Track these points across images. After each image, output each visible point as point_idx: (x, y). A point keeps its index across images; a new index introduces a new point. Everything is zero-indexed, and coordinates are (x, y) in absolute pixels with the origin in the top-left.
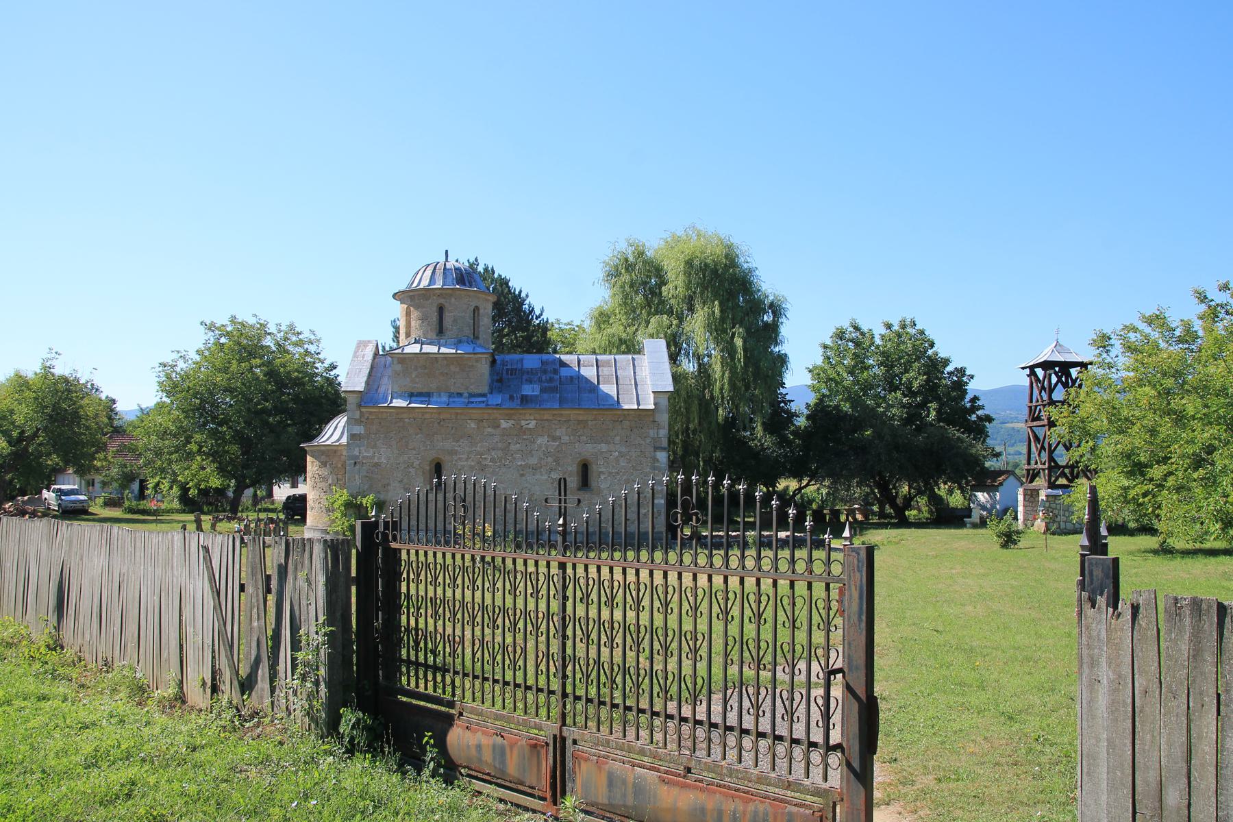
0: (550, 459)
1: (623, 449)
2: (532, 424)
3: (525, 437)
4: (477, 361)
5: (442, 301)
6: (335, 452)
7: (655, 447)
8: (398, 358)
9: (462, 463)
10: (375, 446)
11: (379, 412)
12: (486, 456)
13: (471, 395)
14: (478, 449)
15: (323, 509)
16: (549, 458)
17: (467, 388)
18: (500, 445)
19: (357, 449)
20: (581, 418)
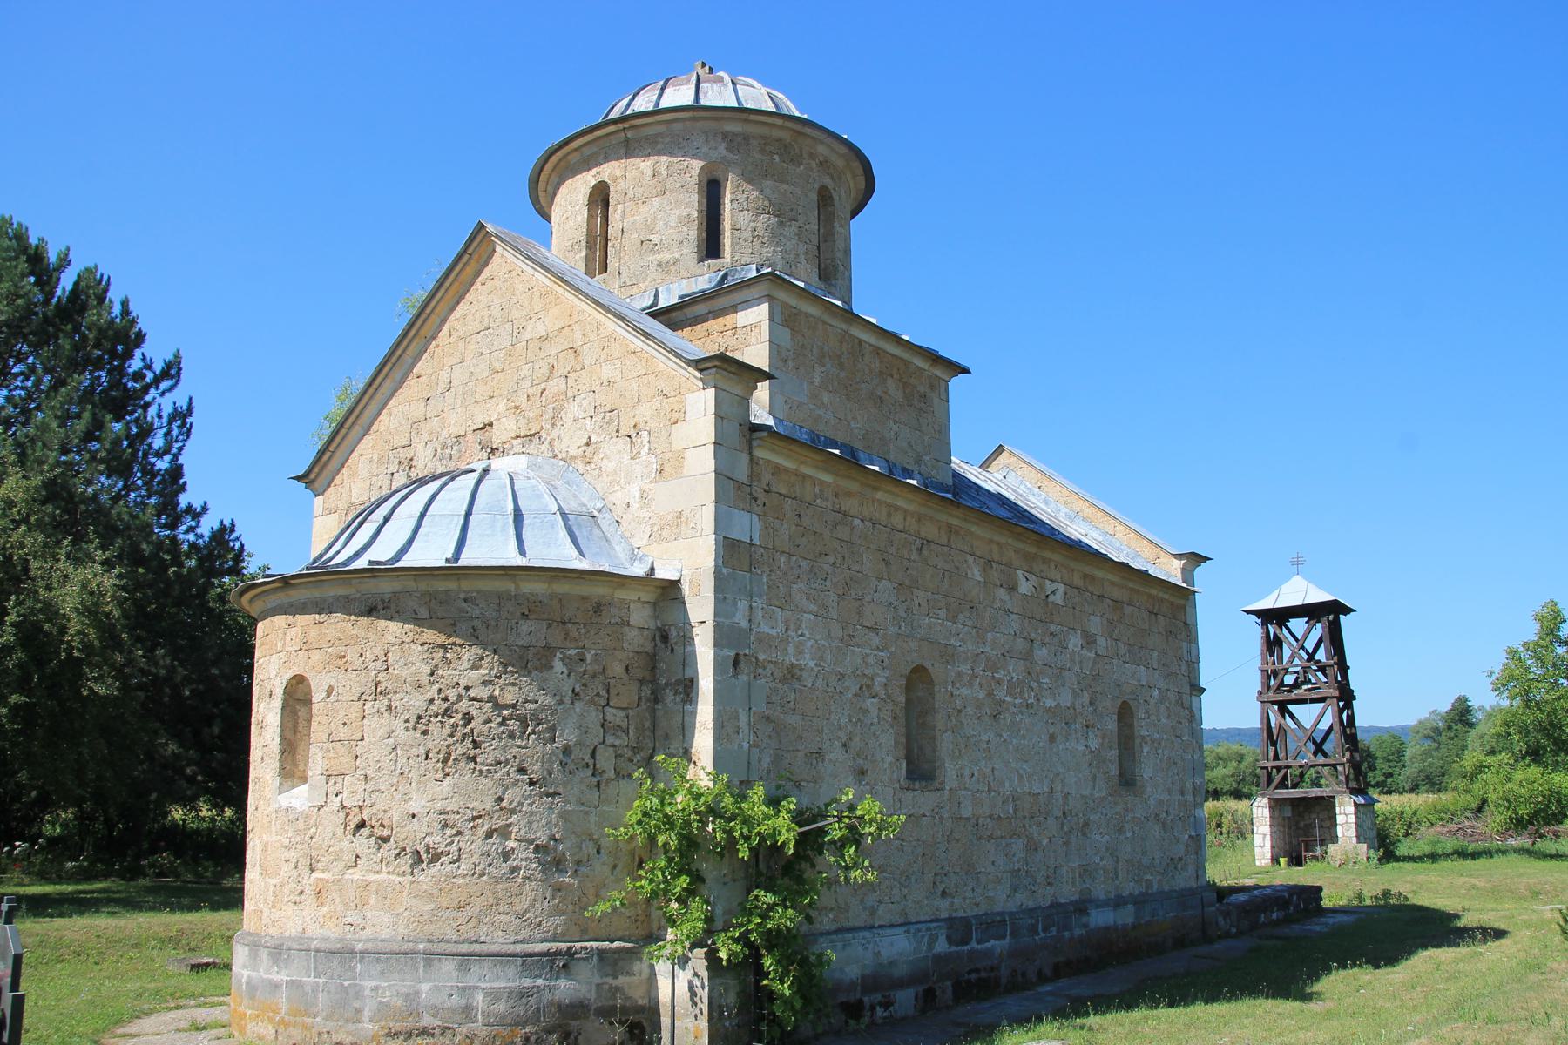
0: (1086, 697)
1: (1163, 686)
2: (1058, 599)
3: (1053, 628)
5: (828, 181)
6: (598, 608)
7: (1191, 686)
8: (785, 305)
9: (965, 691)
14: (987, 649)
15: (523, 857)
16: (1085, 692)
17: (918, 461)
18: (1021, 644)
19: (743, 605)
20: (1117, 594)
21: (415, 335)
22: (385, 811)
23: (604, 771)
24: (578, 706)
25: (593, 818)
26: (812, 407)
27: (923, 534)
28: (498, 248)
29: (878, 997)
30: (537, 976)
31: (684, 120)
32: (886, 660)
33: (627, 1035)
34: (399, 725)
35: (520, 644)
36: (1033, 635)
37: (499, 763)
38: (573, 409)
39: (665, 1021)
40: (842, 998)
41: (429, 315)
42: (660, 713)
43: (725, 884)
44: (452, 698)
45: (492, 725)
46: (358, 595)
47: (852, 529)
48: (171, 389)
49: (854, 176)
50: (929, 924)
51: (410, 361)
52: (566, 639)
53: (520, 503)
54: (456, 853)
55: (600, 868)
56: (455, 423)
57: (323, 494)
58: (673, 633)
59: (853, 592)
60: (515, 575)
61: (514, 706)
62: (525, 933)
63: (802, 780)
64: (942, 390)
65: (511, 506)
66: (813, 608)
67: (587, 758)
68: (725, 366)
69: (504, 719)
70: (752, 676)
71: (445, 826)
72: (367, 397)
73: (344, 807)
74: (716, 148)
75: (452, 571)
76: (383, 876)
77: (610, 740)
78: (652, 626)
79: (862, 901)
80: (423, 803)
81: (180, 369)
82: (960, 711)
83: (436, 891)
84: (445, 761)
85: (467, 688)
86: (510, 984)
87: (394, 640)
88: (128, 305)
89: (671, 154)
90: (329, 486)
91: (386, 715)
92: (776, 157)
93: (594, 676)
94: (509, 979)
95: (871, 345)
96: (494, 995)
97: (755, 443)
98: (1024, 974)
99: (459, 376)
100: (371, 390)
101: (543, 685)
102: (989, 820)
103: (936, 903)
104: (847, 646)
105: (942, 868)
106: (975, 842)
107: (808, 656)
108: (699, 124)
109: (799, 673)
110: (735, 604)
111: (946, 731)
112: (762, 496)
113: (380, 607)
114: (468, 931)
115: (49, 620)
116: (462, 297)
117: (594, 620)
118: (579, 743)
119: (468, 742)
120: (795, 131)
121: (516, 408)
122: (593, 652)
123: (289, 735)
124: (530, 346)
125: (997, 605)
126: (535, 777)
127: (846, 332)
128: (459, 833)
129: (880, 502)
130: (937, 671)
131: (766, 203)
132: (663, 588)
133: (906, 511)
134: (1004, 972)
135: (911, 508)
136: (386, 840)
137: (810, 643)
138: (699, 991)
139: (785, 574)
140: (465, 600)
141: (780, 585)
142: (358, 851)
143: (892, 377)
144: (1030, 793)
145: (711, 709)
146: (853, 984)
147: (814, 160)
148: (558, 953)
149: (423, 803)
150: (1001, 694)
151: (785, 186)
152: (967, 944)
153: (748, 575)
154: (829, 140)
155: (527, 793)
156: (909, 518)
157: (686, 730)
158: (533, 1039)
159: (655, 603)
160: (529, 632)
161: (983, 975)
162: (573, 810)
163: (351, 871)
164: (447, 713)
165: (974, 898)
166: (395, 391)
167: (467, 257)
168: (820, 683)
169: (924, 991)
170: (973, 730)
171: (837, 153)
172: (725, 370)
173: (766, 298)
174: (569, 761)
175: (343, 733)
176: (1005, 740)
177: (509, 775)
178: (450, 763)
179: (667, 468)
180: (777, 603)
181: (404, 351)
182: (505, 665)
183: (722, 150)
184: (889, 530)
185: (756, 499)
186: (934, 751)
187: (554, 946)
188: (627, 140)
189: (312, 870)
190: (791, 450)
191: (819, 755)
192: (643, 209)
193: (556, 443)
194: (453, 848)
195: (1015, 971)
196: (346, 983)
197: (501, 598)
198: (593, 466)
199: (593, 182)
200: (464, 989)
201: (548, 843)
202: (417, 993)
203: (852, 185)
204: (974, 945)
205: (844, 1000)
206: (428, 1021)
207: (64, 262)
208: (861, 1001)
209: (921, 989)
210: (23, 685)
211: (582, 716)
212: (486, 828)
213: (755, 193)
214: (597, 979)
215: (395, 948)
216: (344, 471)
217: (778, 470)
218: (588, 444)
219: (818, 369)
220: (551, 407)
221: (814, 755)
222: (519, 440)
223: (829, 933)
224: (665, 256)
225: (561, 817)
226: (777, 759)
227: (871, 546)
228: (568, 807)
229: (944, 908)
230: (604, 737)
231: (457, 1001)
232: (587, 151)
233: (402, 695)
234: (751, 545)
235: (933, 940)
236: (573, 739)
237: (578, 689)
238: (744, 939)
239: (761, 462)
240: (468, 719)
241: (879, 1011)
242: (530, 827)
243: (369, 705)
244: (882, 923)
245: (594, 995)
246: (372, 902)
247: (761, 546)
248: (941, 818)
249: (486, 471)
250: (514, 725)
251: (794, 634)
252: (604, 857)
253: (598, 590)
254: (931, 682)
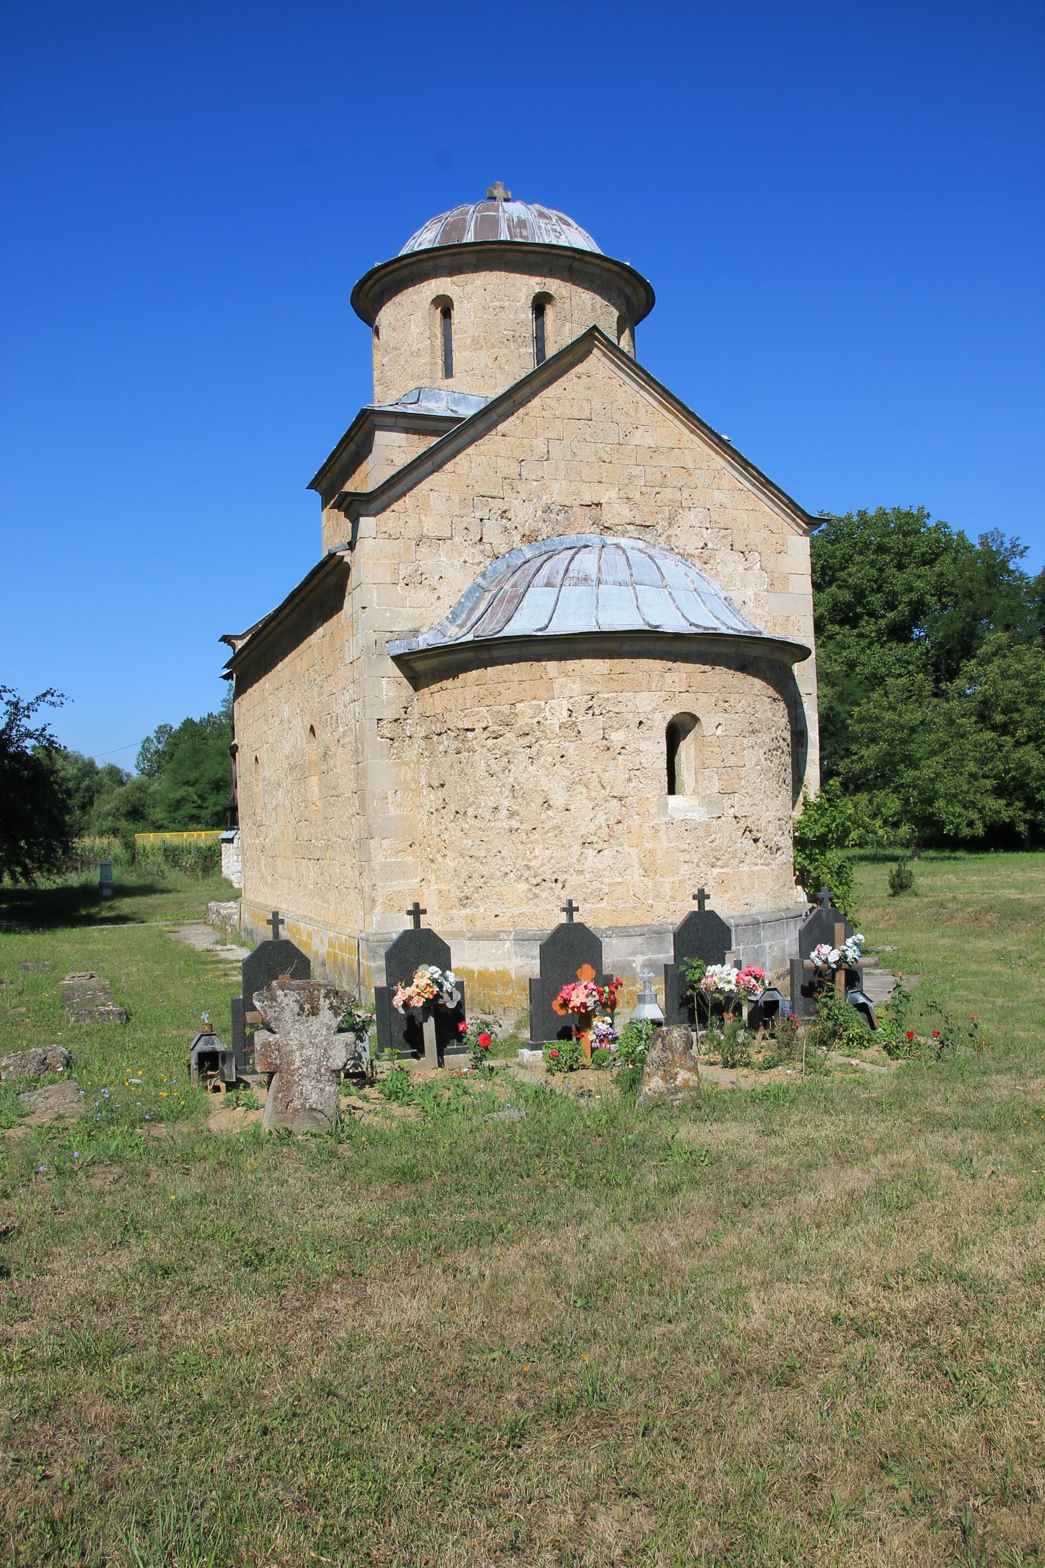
28: (595, 351)
57: (375, 515)
87: (758, 693)
90: (384, 509)
175: (732, 760)
179: (776, 583)
193: (673, 539)
196: (756, 947)
199: (538, 290)
216: (407, 498)
218: (703, 548)
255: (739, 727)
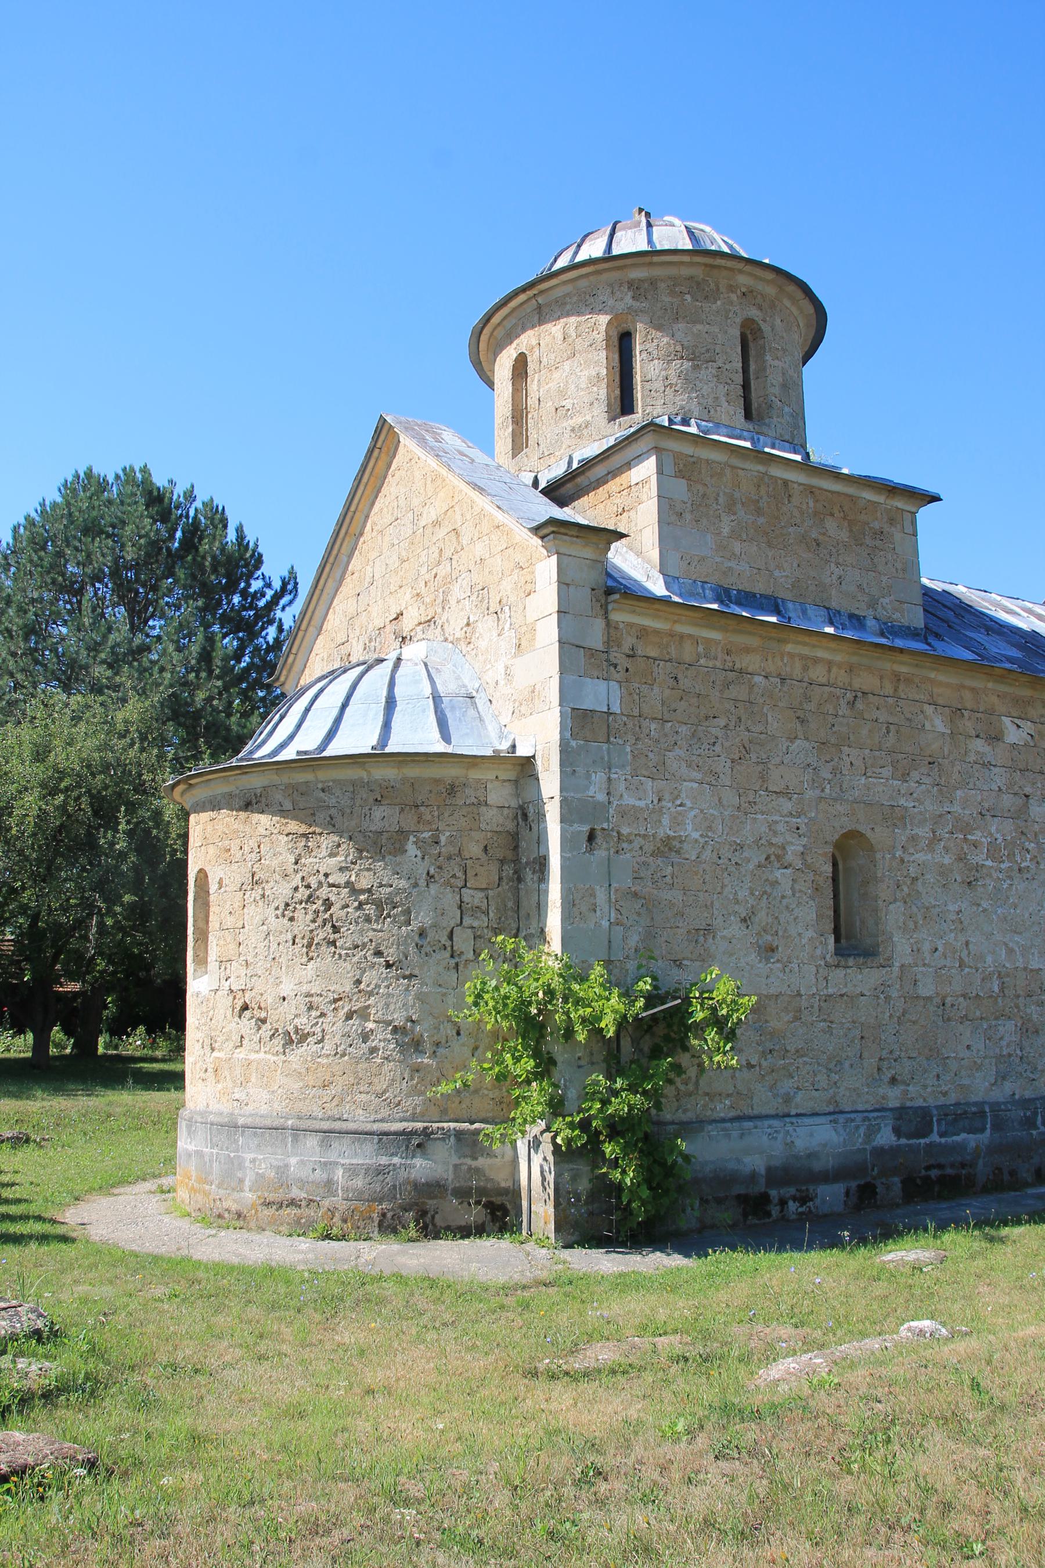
4: (892, 521)
5: (754, 313)
6: (452, 790)
8: (677, 456)
9: (920, 857)
10: (659, 771)
11: (671, 635)
12: (976, 836)
13: (888, 629)
14: (956, 808)
17: (873, 604)
18: (1007, 801)
19: (599, 777)
21: (346, 533)
22: (262, 995)
23: (462, 953)
24: (434, 888)
25: (451, 1000)
26: (718, 560)
27: (856, 685)
29: (792, 1191)
30: (392, 1155)
31: (587, 275)
32: (803, 827)
33: (489, 1217)
34: (270, 912)
35: (373, 829)
36: (1028, 790)
37: (356, 947)
38: (457, 591)
39: (525, 1204)
40: (739, 1190)
41: (355, 512)
42: (522, 893)
43: (579, 1067)
44: (314, 886)
45: (349, 910)
46: (237, 792)
47: (752, 687)
48: (291, 602)
49: (794, 301)
50: (866, 1114)
51: (345, 559)
52: (419, 822)
53: (397, 691)
54: (320, 1034)
55: (460, 1048)
56: (378, 617)
58: (531, 810)
59: (754, 756)
60: (365, 763)
61: (369, 891)
62: (384, 1113)
63: (684, 959)
64: (907, 524)
65: (385, 693)
66: (698, 776)
67: (444, 940)
68: (562, 530)
69: (361, 904)
70: (612, 851)
71: (310, 1008)
72: (315, 598)
73: (232, 991)
74: (622, 299)
75: (307, 762)
76: (262, 1055)
77: (467, 921)
78: (514, 804)
79: (771, 1088)
80: (292, 986)
81: (296, 584)
82: (915, 880)
83: (303, 1070)
84: (309, 946)
85: (326, 875)
86: (367, 1161)
87: (264, 832)
88: (242, 531)
89: (579, 314)
91: (261, 903)
92: (688, 297)
93: (449, 858)
94: (366, 1156)
95: (800, 484)
96: (352, 1171)
97: (610, 607)
98: (1013, 1173)
99: (379, 570)
100: (317, 592)
101: (397, 869)
102: (961, 999)
103: (881, 1091)
104: (746, 814)
105: (891, 1052)
106: (940, 1023)
107: (690, 828)
108: (605, 277)
109: (678, 845)
110: (588, 776)
111: (895, 900)
112: (623, 662)
113: (254, 801)
114: (332, 1110)
115: (157, 826)
116: (379, 491)
117: (448, 802)
118: (434, 926)
119: (328, 927)
120: (706, 265)
121: (418, 595)
122: (448, 834)
123: (201, 924)
124: (426, 532)
125: (972, 758)
126: (391, 959)
127: (765, 474)
128: (323, 1015)
129: (791, 656)
130: (878, 835)
131: (679, 348)
132: (522, 765)
133: (830, 664)
134: (982, 1169)
135: (838, 658)
136: (264, 1021)
137: (693, 813)
138: (547, 1174)
139: (657, 741)
140: (323, 790)
141: (650, 754)
142: (243, 1032)
143: (832, 515)
144: (1025, 969)
145: (559, 886)
146: (753, 1176)
147: (732, 292)
148: (413, 1133)
149: (292, 986)
150: (979, 858)
151: (699, 327)
152: (924, 1136)
153: (605, 746)
154: (748, 268)
155: (384, 975)
156: (834, 670)
157: (541, 908)
158: (389, 1215)
159: (516, 781)
160: (383, 817)
161: (949, 1171)
162: (430, 992)
163: (238, 1050)
164: (310, 899)
165: (940, 1086)
166: (337, 591)
167: (376, 451)
168: (707, 854)
169: (859, 1186)
170: (935, 899)
171: (761, 279)
172: (566, 534)
173: (653, 451)
174: (425, 944)
175: (230, 921)
176: (985, 910)
177: (366, 958)
178: (313, 947)
179: (524, 643)
180: (646, 774)
181: (339, 551)
182: (360, 851)
183: (628, 299)
184: (805, 685)
185: (615, 666)
186: (877, 924)
187: (410, 1126)
188: (539, 307)
189: (213, 1049)
190: (657, 610)
191: (708, 930)
192: (556, 375)
193: (445, 627)
194: (318, 1029)
195: (1000, 1169)
196: (232, 1155)
197: (355, 785)
198: (471, 645)
199: (515, 355)
200: (325, 1164)
201: (406, 1024)
202: (287, 1166)
203: (796, 312)
204: (935, 1137)
205: (742, 1192)
206: (296, 1193)
207: (190, 496)
208: (765, 1198)
209: (853, 1184)
210: (137, 886)
211: (437, 898)
212: (346, 1010)
213: (665, 340)
214: (455, 1160)
215: (268, 1122)
217: (643, 633)
218: (468, 624)
219: (726, 519)
220: (441, 590)
221: (702, 932)
222: (421, 627)
223: (723, 1120)
224: (578, 420)
225: (418, 999)
226: (650, 935)
227: (780, 704)
228: (425, 989)
229: (893, 1097)
230: (461, 918)
231: (319, 1175)
232: (508, 324)
233: (272, 884)
234: (609, 713)
235: (872, 1132)
236: (428, 922)
237: (432, 872)
238: (585, 1125)
239: (621, 626)
240: (328, 904)
241: (792, 1206)
242: (387, 1008)
243: (248, 893)
244: (799, 1111)
245: (451, 1177)
246: (253, 1080)
247: (622, 714)
248: (888, 998)
249: (399, 659)
250: (370, 910)
251: (670, 805)
252: (463, 1038)
253: (450, 772)
254: (871, 849)
255: (239, 880)
